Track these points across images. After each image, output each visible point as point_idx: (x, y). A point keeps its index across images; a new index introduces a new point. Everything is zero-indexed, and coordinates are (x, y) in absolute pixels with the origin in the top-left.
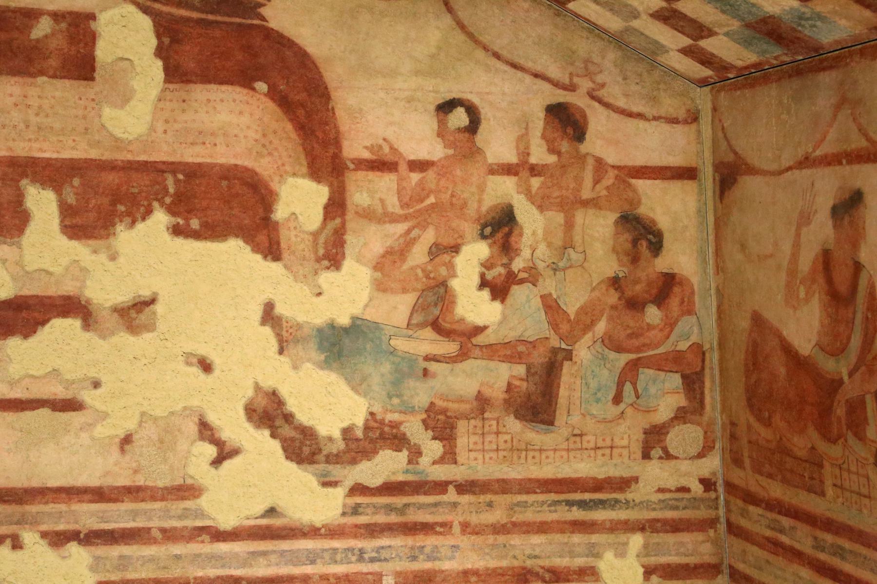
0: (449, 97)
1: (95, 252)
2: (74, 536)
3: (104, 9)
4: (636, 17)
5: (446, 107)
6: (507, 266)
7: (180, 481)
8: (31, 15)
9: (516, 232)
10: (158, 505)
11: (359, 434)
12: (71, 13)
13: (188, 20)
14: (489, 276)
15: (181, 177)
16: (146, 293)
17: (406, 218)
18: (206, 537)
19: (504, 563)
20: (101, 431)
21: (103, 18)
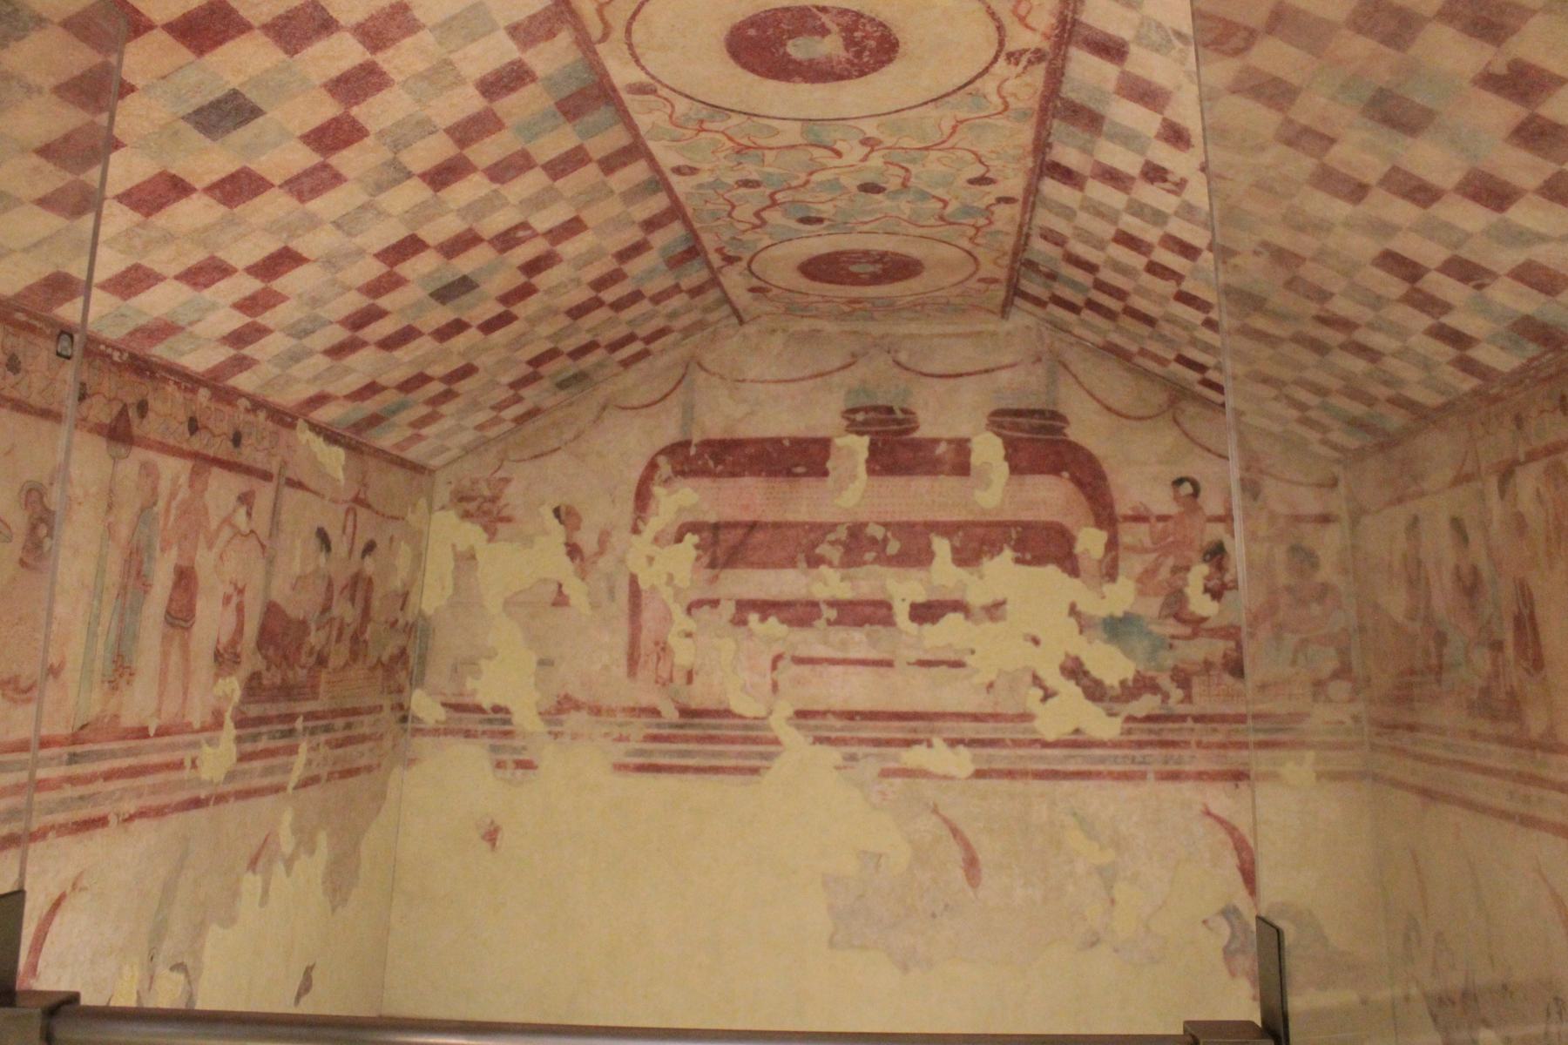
0: (1179, 476)
1: (972, 574)
2: (960, 742)
5: (1178, 482)
6: (1221, 579)
7: (1022, 711)
8: (936, 441)
9: (1225, 560)
10: (1010, 725)
11: (1130, 683)
13: (1020, 439)
14: (1211, 584)
15: (1019, 529)
16: (1000, 598)
17: (1155, 550)
18: (1038, 745)
19: (1225, 768)
20: (977, 680)
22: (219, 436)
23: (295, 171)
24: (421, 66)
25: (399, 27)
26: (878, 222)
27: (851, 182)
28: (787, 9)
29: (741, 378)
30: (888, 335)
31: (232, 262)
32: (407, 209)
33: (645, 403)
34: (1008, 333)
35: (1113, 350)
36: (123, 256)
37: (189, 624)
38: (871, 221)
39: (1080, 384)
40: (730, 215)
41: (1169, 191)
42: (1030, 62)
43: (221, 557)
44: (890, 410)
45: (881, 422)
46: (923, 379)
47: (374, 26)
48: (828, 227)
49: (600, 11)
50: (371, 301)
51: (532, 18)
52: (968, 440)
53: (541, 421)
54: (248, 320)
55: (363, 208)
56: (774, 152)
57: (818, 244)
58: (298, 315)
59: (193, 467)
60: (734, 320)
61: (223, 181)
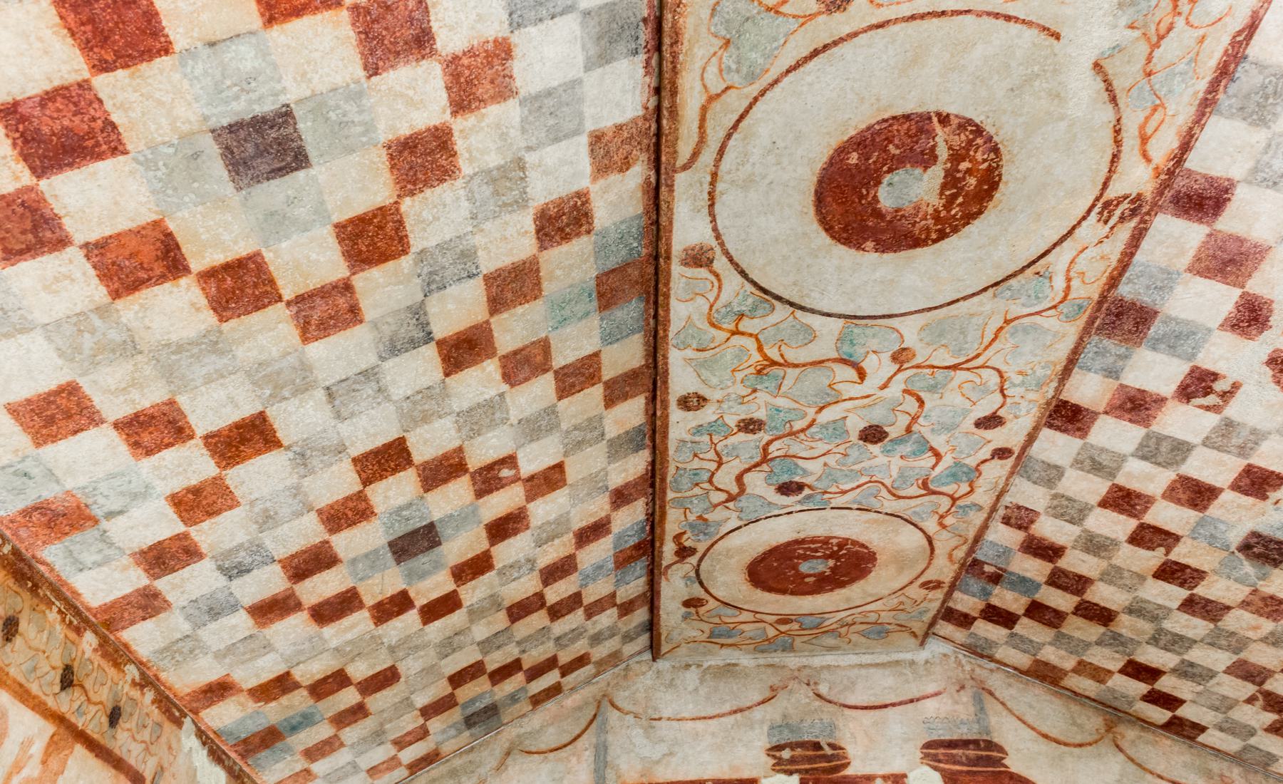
3: (911, 771)
4: (1252, 735)
12: (892, 775)
13: (961, 772)
21: (911, 776)
23: (313, 283)
24: (493, 160)
25: (492, 82)
26: (858, 491)
27: (856, 424)
28: (907, 117)
29: (657, 717)
30: (805, 667)
31: (193, 419)
32: (409, 393)
33: (553, 746)
34: (927, 662)
35: (1045, 674)
36: (60, 362)
38: (853, 489)
39: (1010, 711)
40: (710, 481)
41: (1208, 408)
42: (1122, 219)
44: (817, 746)
45: (810, 760)
46: (847, 711)
47: (468, 67)
48: (809, 497)
49: (704, 109)
50: (327, 537)
51: (619, 128)
52: (905, 776)
53: (435, 770)
54: (180, 528)
55: (368, 374)
56: (798, 371)
57: (778, 531)
58: (241, 537)
60: (647, 656)
61: (227, 267)
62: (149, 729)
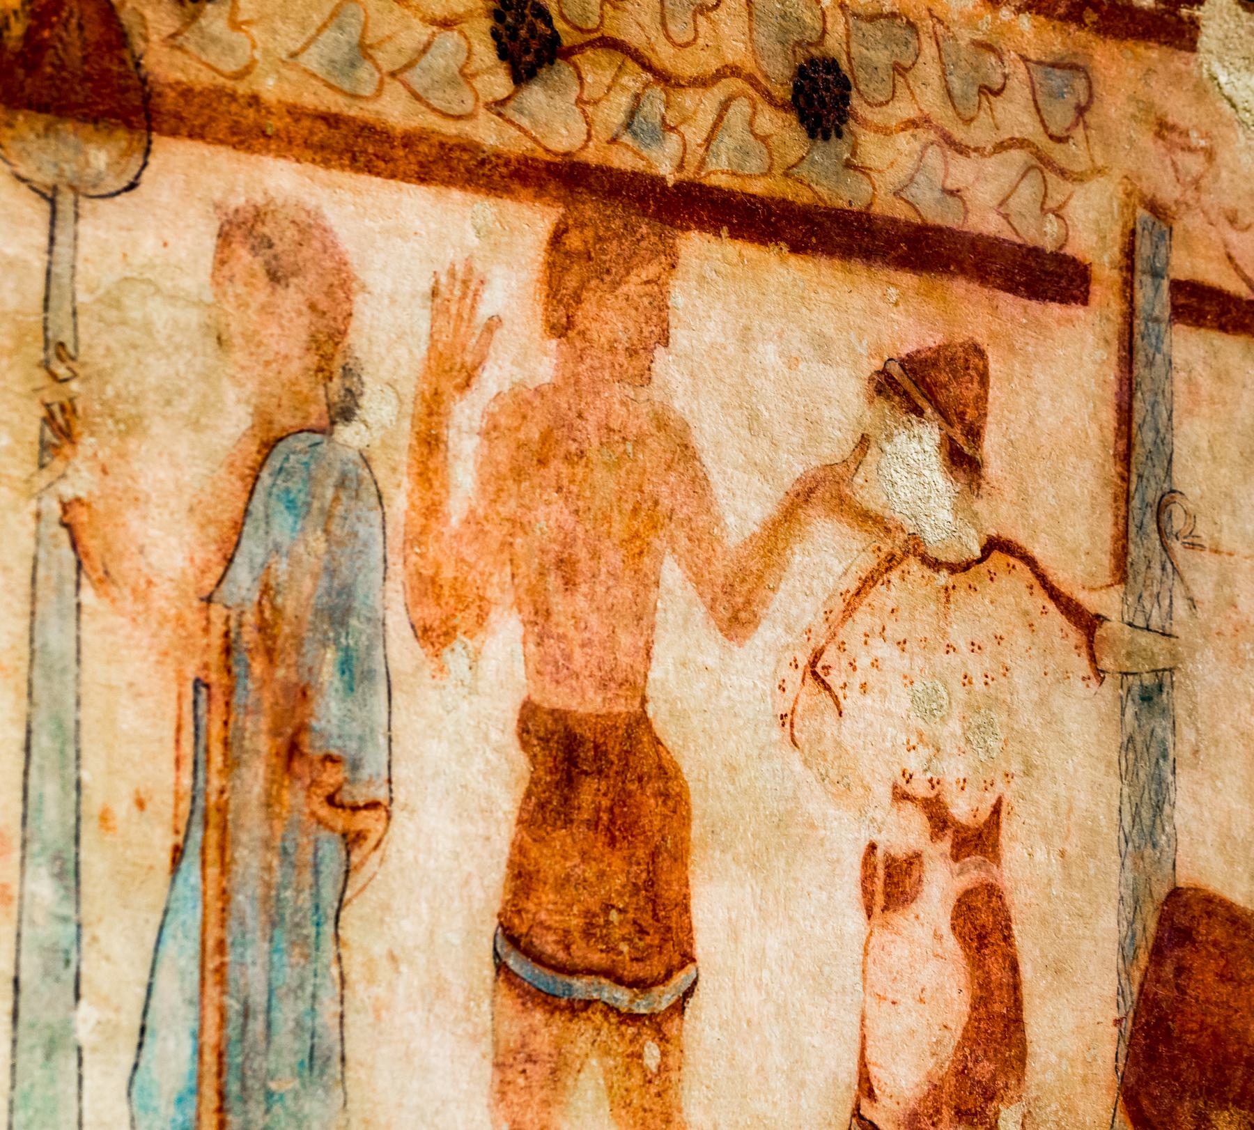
22: (702, 83)
37: (664, 998)
43: (816, 672)
59: (557, 239)
62: (1019, 92)
